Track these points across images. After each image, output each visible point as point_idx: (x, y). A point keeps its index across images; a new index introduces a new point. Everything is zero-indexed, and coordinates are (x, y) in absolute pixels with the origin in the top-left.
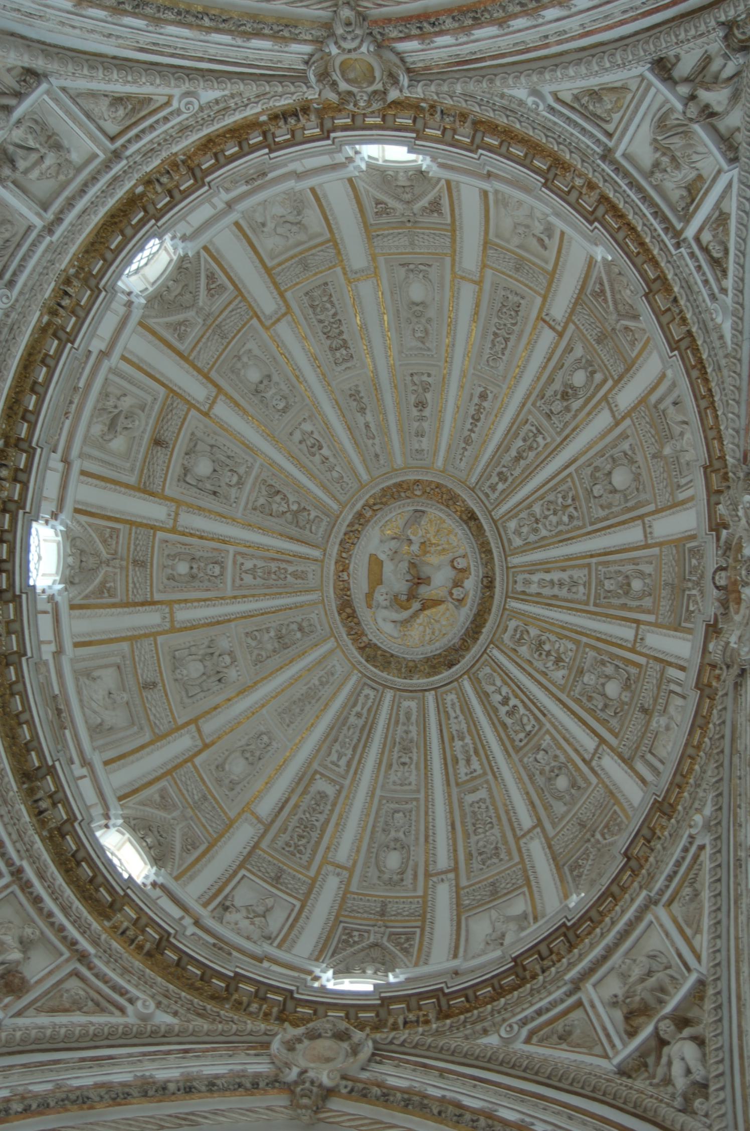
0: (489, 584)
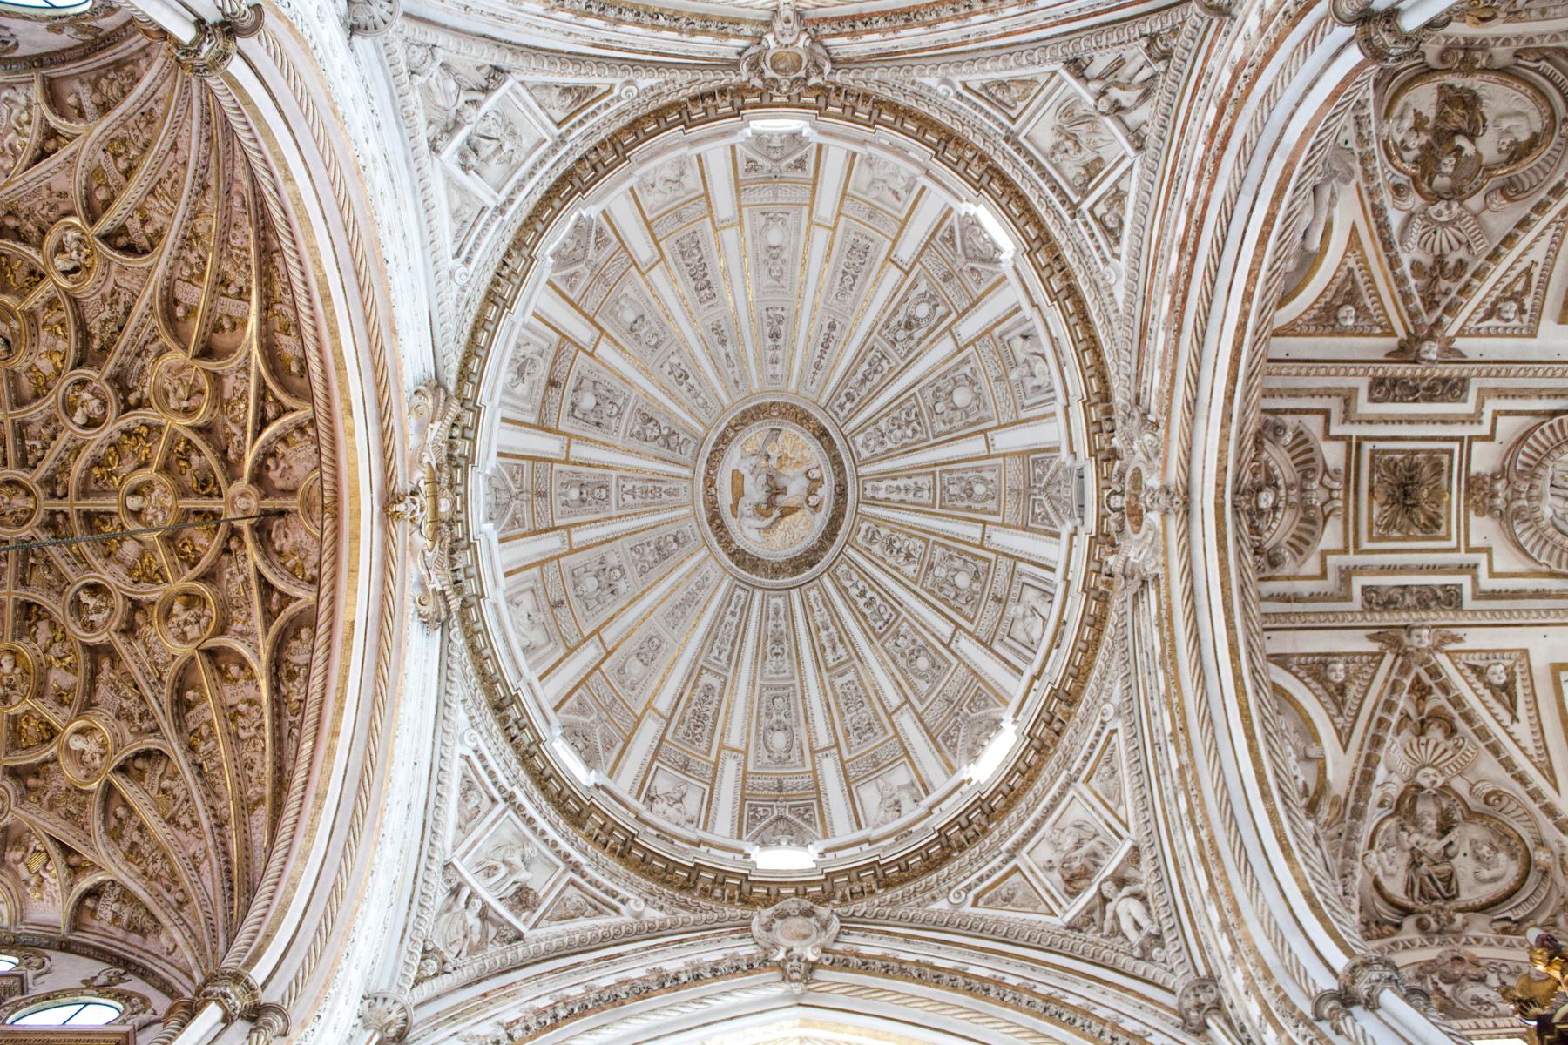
0: (841, 492)
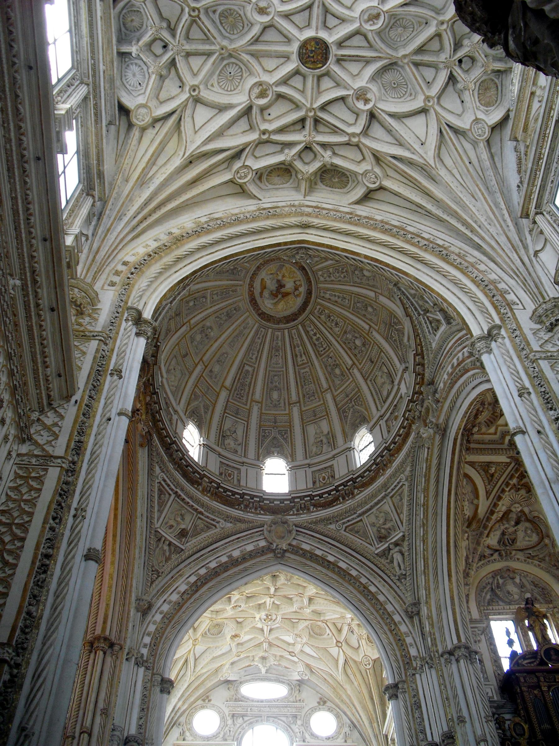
0: (309, 293)
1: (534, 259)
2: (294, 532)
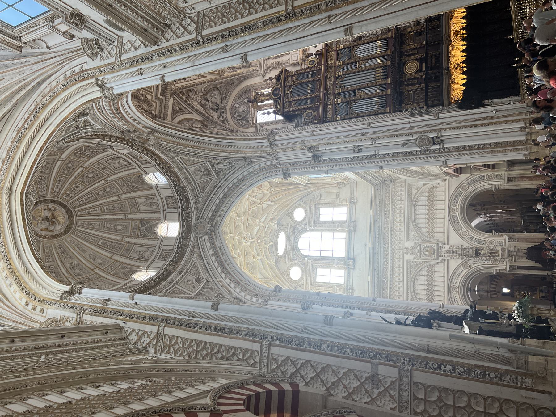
0: (54, 201)
1: (52, 50)
2: (202, 220)
